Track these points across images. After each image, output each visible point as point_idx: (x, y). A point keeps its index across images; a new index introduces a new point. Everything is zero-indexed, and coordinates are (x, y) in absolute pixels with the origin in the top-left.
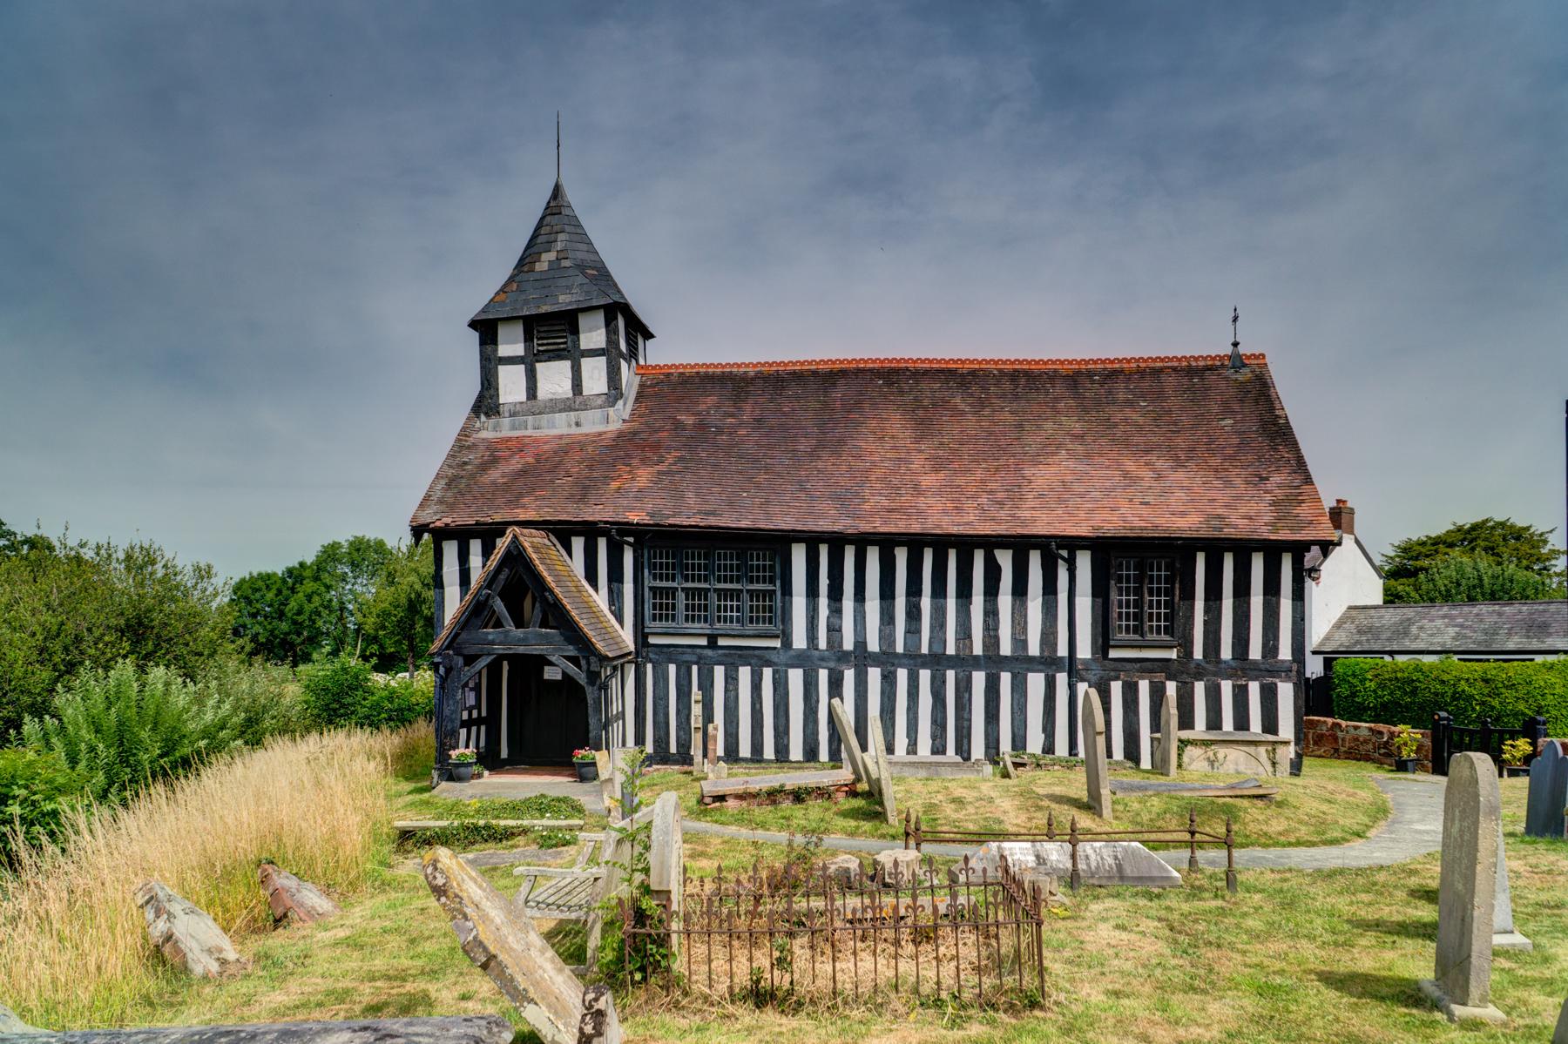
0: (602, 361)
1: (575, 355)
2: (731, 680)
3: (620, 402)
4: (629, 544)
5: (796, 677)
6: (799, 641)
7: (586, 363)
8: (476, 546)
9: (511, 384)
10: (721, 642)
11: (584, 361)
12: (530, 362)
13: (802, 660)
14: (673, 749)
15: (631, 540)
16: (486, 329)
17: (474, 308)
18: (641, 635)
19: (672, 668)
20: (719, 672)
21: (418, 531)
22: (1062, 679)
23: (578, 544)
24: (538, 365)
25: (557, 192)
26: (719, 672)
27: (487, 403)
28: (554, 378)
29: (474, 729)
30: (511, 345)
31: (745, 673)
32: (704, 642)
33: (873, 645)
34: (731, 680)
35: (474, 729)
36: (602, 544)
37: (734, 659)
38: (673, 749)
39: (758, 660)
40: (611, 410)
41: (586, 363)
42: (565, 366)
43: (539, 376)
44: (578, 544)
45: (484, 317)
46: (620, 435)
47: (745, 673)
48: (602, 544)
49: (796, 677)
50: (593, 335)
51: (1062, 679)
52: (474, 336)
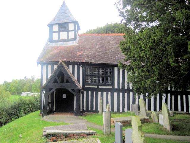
0: (73, 32)
2: (102, 95)
3: (76, 40)
4: (81, 66)
6: (116, 87)
7: (70, 32)
8: (50, 67)
10: (100, 87)
12: (59, 32)
14: (90, 109)
16: (50, 26)
17: (49, 22)
18: (83, 85)
19: (90, 92)
21: (38, 63)
22: (169, 95)
23: (71, 66)
24: (61, 33)
27: (51, 40)
28: (63, 35)
29: (49, 104)
30: (55, 28)
34: (102, 95)
35: (49, 104)
36: (76, 66)
37: (103, 90)
38: (90, 109)
39: (107, 90)
41: (70, 32)
42: (66, 33)
44: (71, 66)
45: (51, 23)
46: (77, 46)
47: (105, 93)
48: (76, 66)
49: (115, 94)
50: (71, 27)
51: (169, 95)
52: (48, 29)
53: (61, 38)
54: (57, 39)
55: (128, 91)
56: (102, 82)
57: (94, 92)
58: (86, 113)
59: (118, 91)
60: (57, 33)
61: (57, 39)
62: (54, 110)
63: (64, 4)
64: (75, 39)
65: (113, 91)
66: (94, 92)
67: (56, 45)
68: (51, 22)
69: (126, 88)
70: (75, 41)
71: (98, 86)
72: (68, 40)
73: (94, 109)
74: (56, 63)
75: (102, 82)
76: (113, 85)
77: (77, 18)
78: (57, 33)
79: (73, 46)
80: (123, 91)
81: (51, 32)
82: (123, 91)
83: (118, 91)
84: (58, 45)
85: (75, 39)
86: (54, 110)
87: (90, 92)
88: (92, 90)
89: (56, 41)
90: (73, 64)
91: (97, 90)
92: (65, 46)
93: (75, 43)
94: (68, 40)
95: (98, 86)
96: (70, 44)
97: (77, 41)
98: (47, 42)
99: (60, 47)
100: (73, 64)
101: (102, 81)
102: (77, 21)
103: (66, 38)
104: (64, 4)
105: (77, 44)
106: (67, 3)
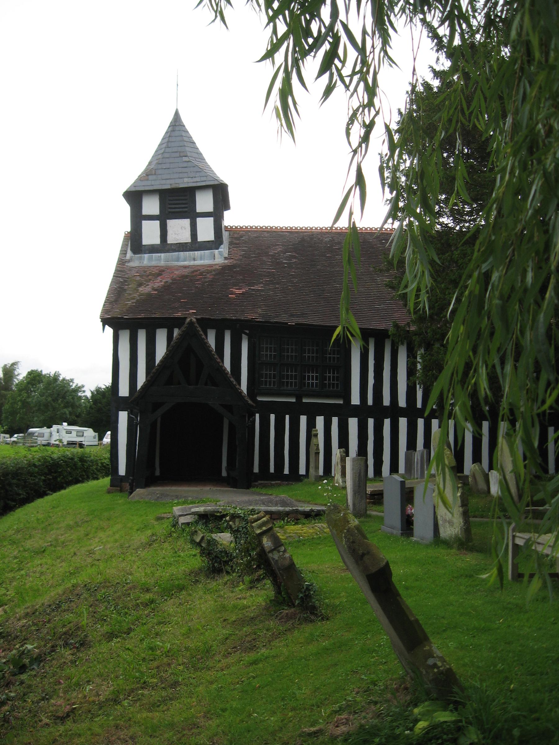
1: (191, 214)
4: (246, 334)
5: (353, 423)
6: (355, 400)
7: (199, 220)
9: (151, 233)
11: (199, 220)
13: (356, 411)
14: (272, 470)
15: (247, 332)
16: (134, 197)
19: (273, 417)
20: (303, 419)
25: (177, 114)
26: (303, 419)
28: (179, 230)
30: (151, 206)
31: (320, 421)
32: (293, 400)
33: (402, 402)
34: (311, 425)
38: (272, 470)
39: (328, 412)
40: (216, 252)
41: (199, 220)
42: (186, 223)
43: (169, 228)
45: (134, 189)
47: (320, 421)
49: (353, 423)
50: (204, 202)
53: (171, 239)
54: (157, 241)
55: (394, 412)
56: (312, 383)
57: (287, 417)
58: (260, 482)
59: (362, 413)
60: (157, 223)
61: (157, 241)
62: (158, 473)
63: (177, 124)
64: (217, 243)
65: (345, 412)
66: (287, 417)
67: (154, 263)
68: (134, 185)
69: (386, 402)
70: (218, 249)
71: (299, 398)
72: (195, 245)
73: (286, 471)
74: (169, 324)
75: (312, 383)
76: (347, 395)
77: (222, 171)
78: (157, 223)
79: (211, 266)
80: (378, 412)
81: (137, 218)
82: (378, 412)
83: (362, 413)
84: (162, 263)
85: (217, 243)
86: (158, 473)
87: (273, 417)
88: (280, 410)
89: (152, 249)
90: (220, 326)
91: (295, 411)
92: (185, 267)
93: (219, 257)
94: (195, 245)
95: (299, 398)
96: (201, 259)
97: (224, 249)
98: (123, 252)
99: (168, 268)
100: (220, 326)
101: (312, 378)
102: (226, 181)
103: (186, 237)
104: (177, 124)
105: (226, 258)
106: (185, 120)
